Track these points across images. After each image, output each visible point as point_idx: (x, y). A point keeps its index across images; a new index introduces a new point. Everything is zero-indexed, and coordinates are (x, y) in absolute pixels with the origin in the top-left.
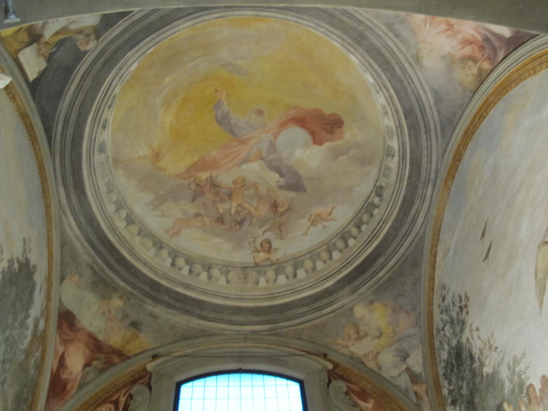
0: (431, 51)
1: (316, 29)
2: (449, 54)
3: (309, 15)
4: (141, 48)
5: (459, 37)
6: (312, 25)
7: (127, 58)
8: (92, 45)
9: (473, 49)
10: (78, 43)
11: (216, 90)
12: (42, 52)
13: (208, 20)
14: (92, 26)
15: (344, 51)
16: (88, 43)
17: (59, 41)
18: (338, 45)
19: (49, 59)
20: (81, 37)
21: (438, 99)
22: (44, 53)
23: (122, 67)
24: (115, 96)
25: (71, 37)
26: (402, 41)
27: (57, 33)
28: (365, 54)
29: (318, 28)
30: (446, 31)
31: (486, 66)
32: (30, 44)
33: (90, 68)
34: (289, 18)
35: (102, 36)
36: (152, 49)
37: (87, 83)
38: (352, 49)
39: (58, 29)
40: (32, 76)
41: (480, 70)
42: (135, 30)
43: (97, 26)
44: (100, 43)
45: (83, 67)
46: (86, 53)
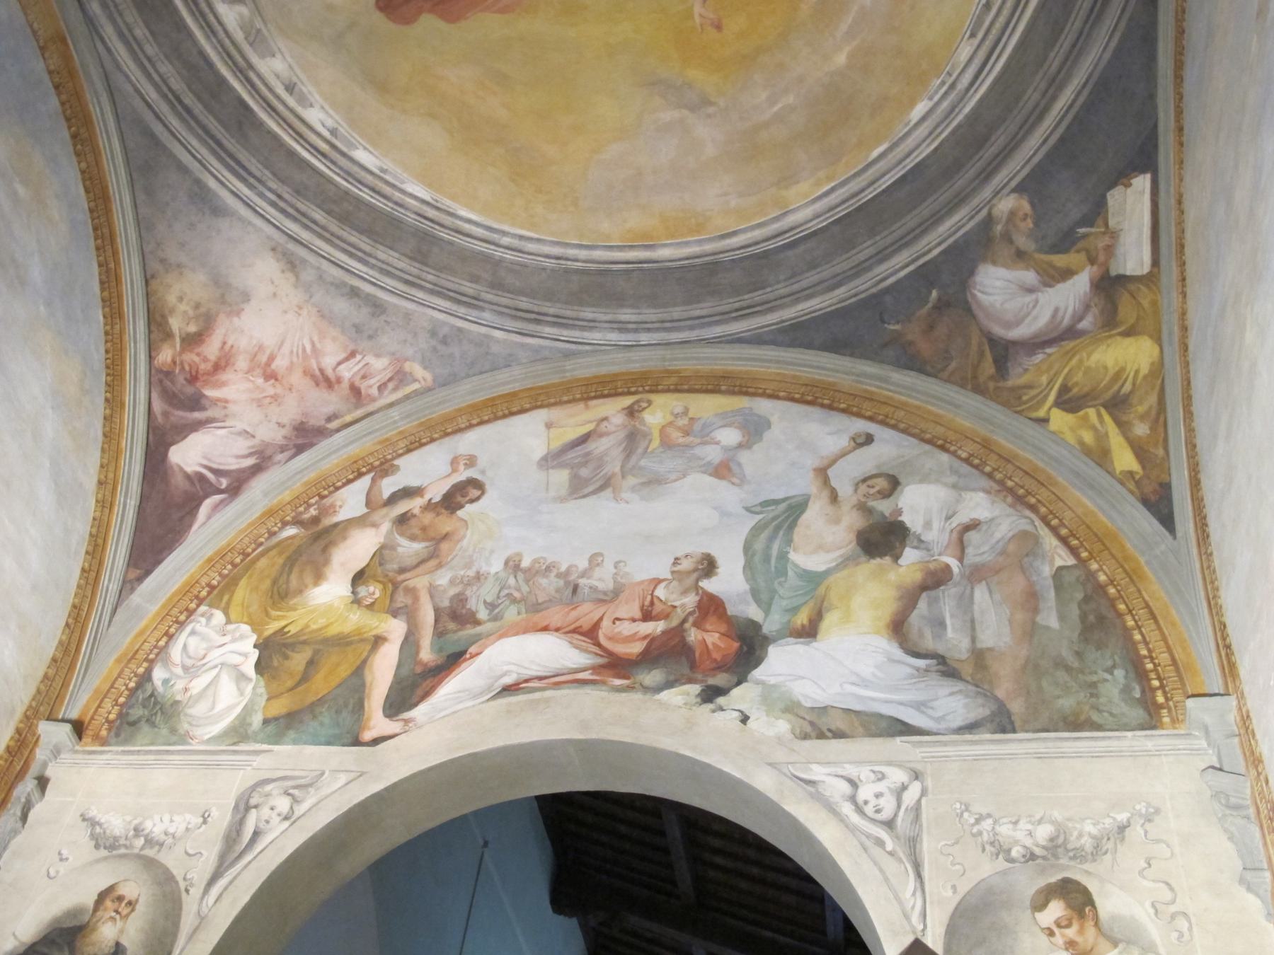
0: (275, 295)
1: (521, 237)
2: (238, 313)
3: (544, 269)
4: (900, 162)
5: (242, 363)
6: (531, 247)
7: (933, 140)
8: (1006, 205)
9: (205, 360)
10: (1030, 223)
11: (719, 27)
12: (1107, 240)
13: (753, 228)
14: (994, 263)
15: (447, 203)
16: (1012, 214)
17: (1065, 251)
18: (463, 213)
19: (1097, 211)
20: (1022, 242)
21: (202, 199)
22: (1104, 233)
23: (946, 117)
24: (973, 35)
25: (1040, 250)
26: (339, 285)
27: (1066, 274)
28: (399, 213)
29: (515, 243)
30: (272, 358)
31: (165, 355)
32: (1123, 279)
33: (1019, 136)
34: (583, 254)
35: (978, 225)
36: (875, 154)
37: (1032, 96)
38: (431, 213)
39: (1060, 286)
40: (1142, 182)
41: (168, 335)
42: (910, 221)
43: (984, 259)
44: (985, 205)
45: (1034, 146)
46: (1019, 189)
